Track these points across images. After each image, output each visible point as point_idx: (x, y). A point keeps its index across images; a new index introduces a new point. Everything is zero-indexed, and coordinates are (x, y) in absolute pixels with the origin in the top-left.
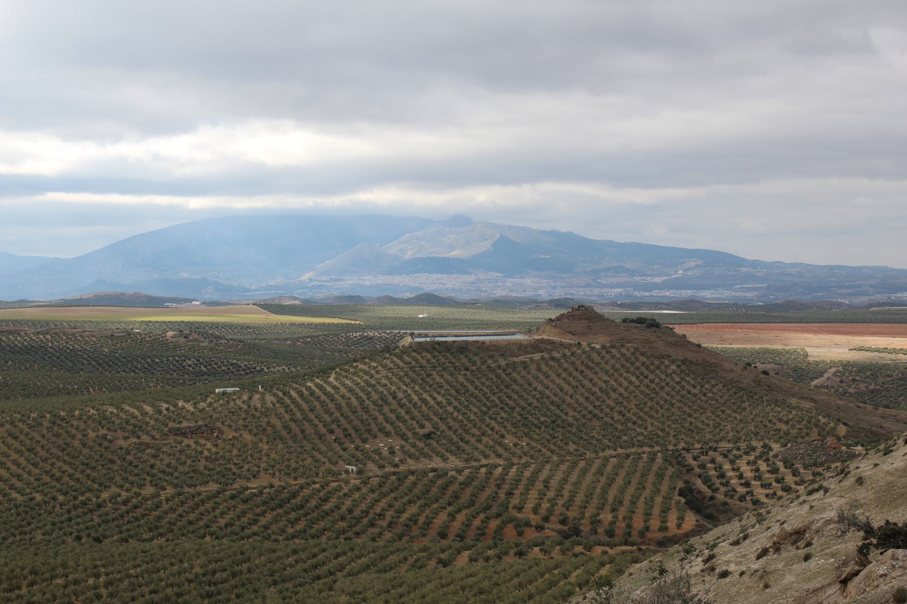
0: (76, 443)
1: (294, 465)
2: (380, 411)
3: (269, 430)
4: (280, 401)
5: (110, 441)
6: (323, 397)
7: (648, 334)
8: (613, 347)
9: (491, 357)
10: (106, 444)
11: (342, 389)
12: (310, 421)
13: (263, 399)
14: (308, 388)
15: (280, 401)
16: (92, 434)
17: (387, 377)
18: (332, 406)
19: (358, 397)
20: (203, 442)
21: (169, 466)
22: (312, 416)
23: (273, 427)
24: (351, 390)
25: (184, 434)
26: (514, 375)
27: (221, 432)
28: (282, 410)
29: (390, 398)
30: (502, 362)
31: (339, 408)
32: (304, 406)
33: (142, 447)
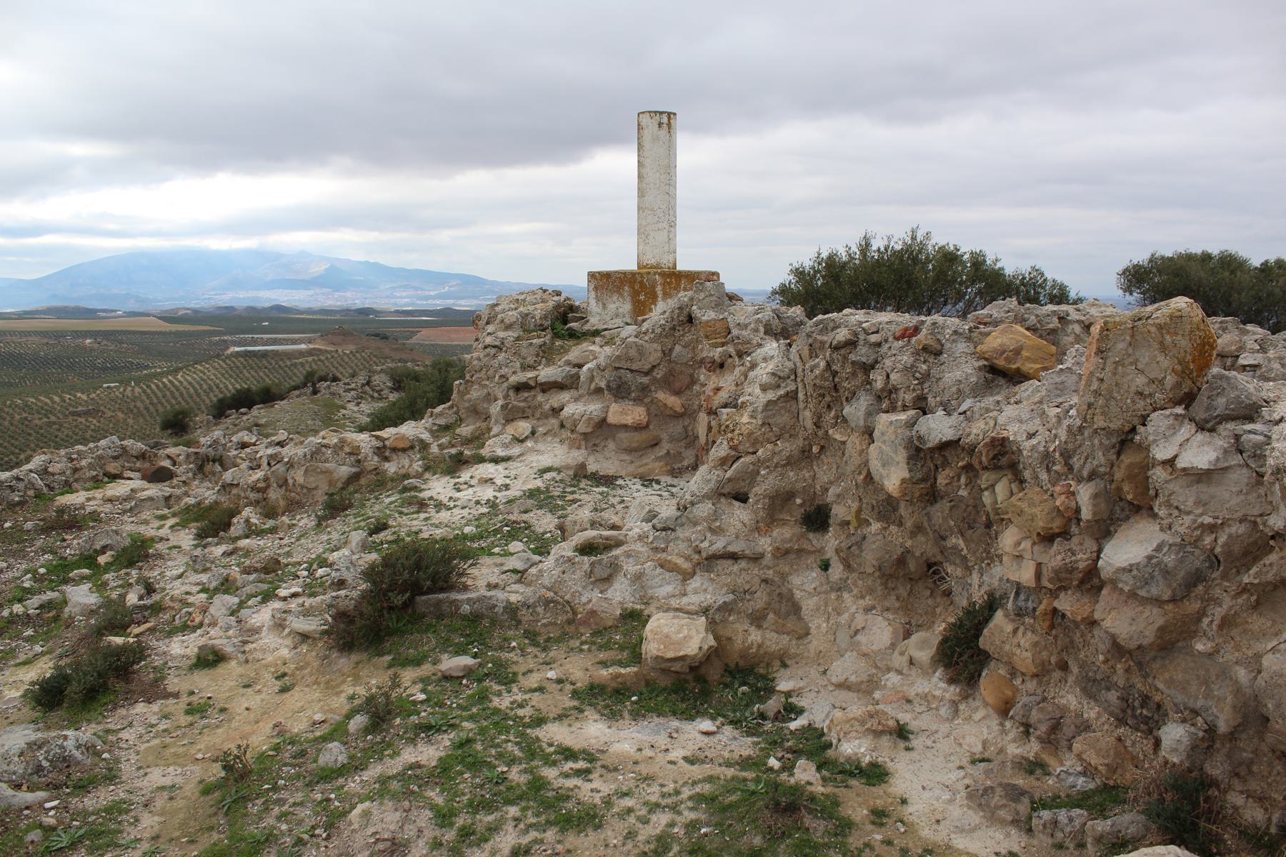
0: (6, 423)
1: (148, 433)
2: (208, 396)
3: (135, 411)
4: (144, 391)
5: (29, 421)
6: (172, 389)
7: (381, 344)
8: (357, 352)
9: (282, 360)
10: (26, 423)
11: (185, 383)
12: (162, 404)
13: (133, 391)
14: (163, 383)
15: (144, 391)
16: (17, 417)
17: (214, 375)
18: (177, 394)
19: (194, 388)
20: (90, 419)
21: (67, 436)
22: (164, 401)
23: (138, 408)
24: (190, 383)
25: (79, 415)
26: (295, 371)
27: (104, 413)
28: (144, 398)
29: (215, 388)
30: (288, 363)
31: (181, 394)
32: (160, 394)
33: (50, 424)
